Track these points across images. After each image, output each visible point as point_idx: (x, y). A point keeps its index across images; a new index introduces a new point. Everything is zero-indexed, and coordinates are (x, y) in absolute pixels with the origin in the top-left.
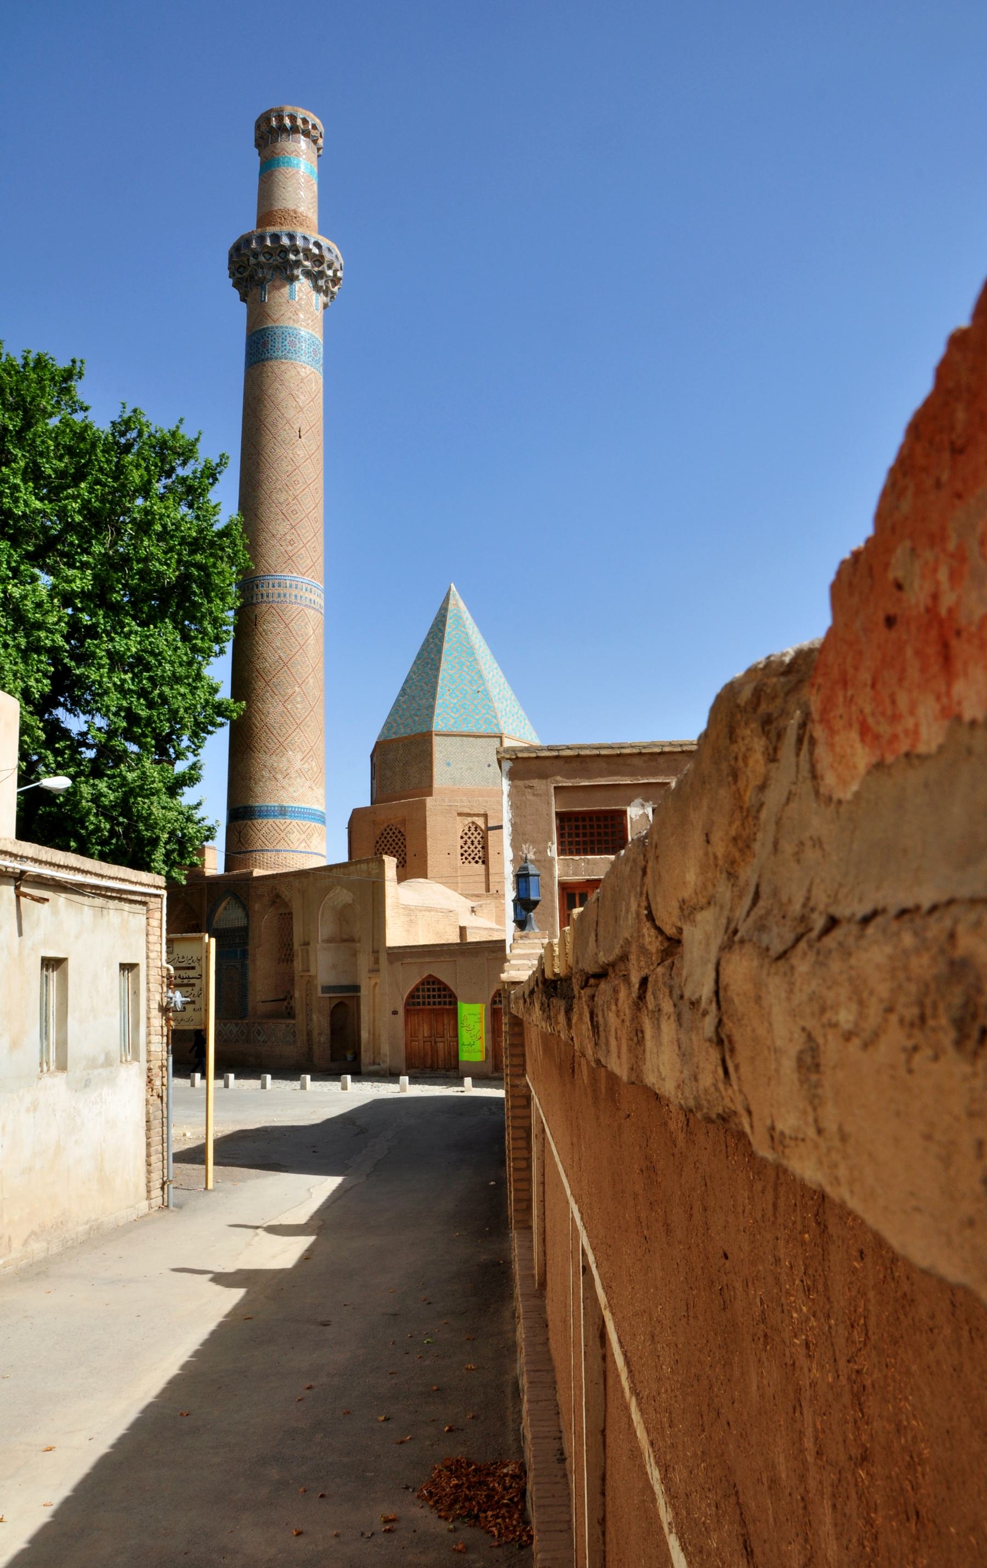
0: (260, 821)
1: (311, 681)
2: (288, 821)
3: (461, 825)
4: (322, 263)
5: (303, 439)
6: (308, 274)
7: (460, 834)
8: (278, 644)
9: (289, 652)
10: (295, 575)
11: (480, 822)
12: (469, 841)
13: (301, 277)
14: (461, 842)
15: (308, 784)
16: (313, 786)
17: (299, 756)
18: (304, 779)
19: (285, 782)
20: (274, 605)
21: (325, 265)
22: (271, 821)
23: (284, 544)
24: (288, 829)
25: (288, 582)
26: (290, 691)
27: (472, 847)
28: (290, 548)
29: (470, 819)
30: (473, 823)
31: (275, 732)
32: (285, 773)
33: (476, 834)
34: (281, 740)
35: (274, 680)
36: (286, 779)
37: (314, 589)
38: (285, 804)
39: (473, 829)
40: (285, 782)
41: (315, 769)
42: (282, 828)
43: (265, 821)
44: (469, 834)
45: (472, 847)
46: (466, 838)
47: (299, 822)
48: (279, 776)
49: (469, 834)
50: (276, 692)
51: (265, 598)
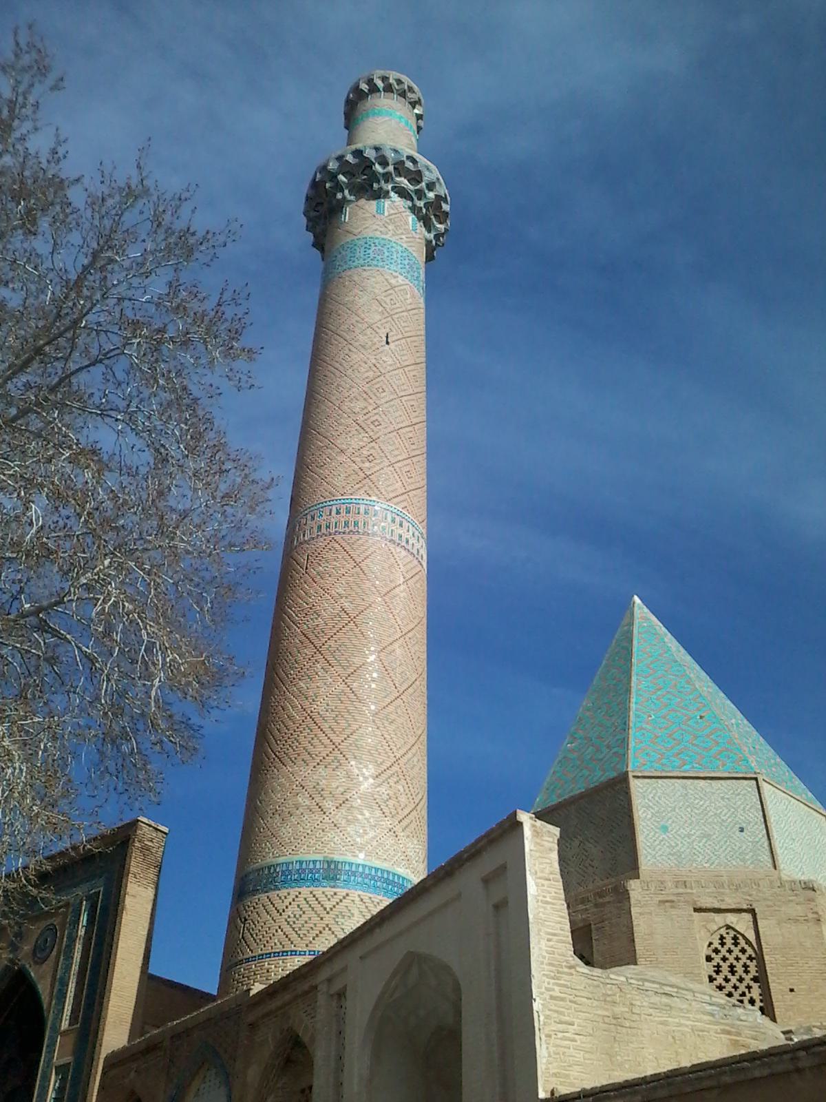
0: (283, 893)
1: (398, 651)
2: (342, 892)
3: (704, 932)
4: (419, 182)
5: (392, 345)
6: (402, 193)
7: (705, 951)
8: (341, 591)
9: (358, 601)
10: (374, 498)
11: (743, 924)
12: (725, 967)
13: (392, 194)
14: (709, 969)
15: (387, 823)
16: (398, 829)
17: (370, 770)
18: (378, 813)
19: (340, 816)
20: (338, 537)
21: (423, 184)
22: (305, 891)
23: (358, 459)
24: (341, 907)
25: (362, 508)
26: (357, 661)
27: (734, 980)
28: (367, 464)
29: (720, 919)
30: (728, 927)
31: (325, 726)
32: (342, 798)
33: (736, 951)
34: (337, 740)
35: (331, 643)
36: (343, 811)
37: (405, 524)
38: (336, 857)
39: (729, 941)
40: (340, 816)
41: (403, 799)
42: (328, 905)
43: (293, 892)
44: (724, 951)
45: (734, 980)
46: (717, 959)
47: (366, 896)
48: (328, 805)
49: (724, 951)
50: (333, 661)
51: (323, 530)
